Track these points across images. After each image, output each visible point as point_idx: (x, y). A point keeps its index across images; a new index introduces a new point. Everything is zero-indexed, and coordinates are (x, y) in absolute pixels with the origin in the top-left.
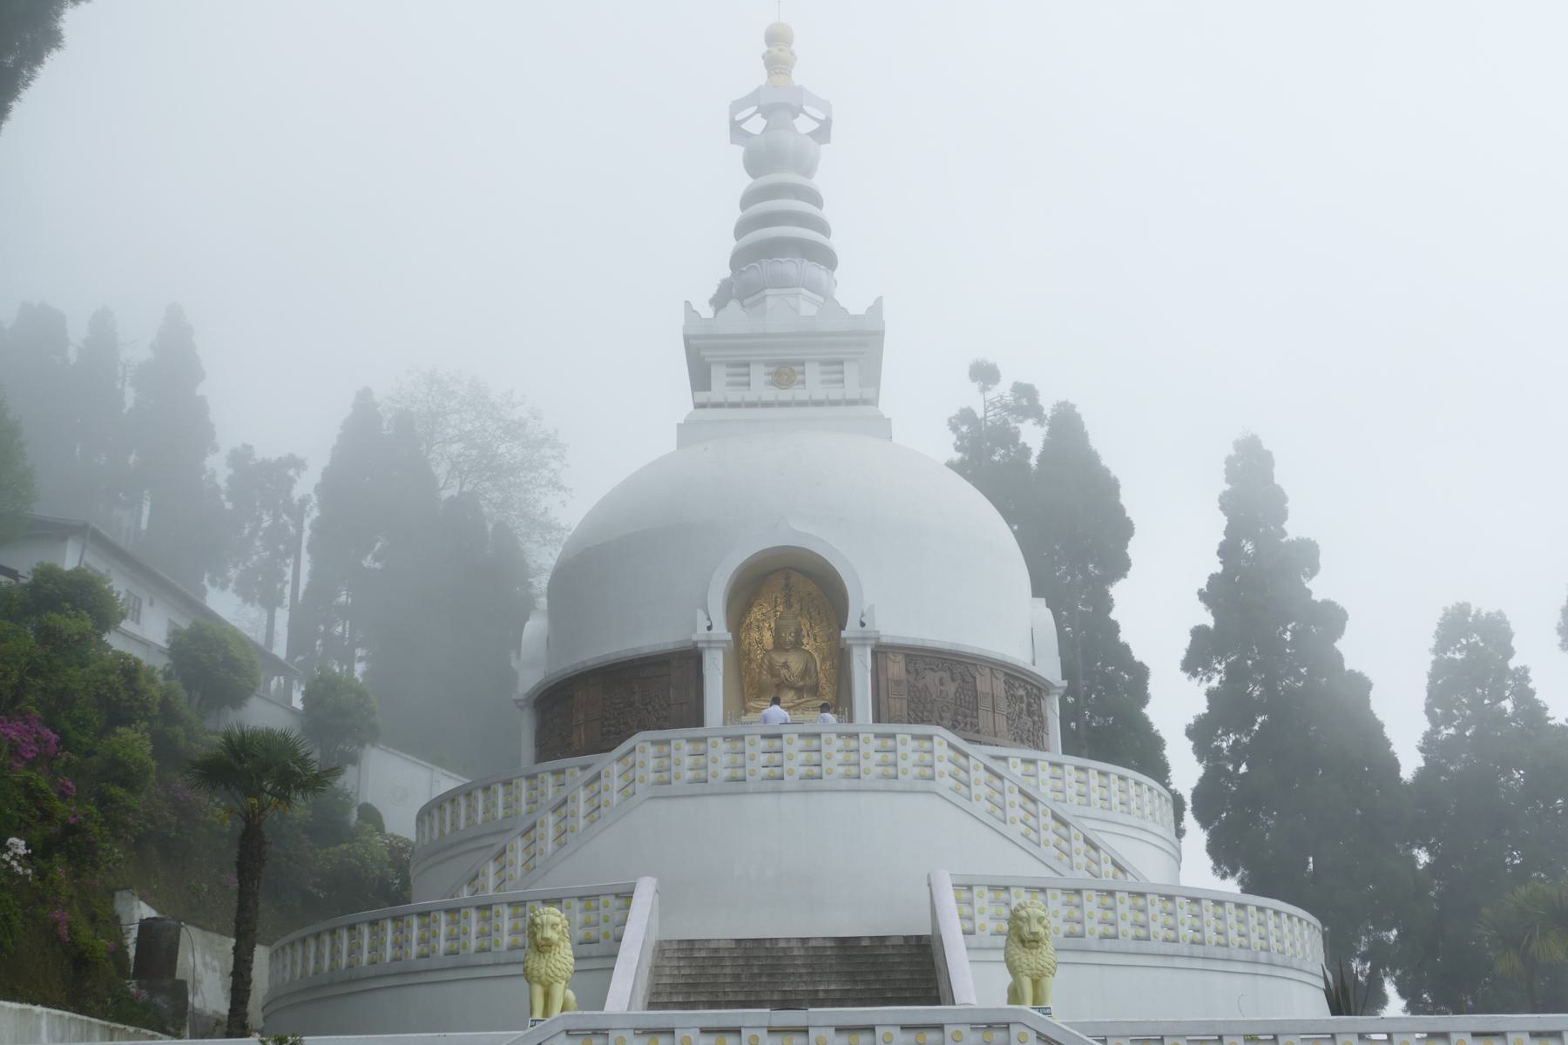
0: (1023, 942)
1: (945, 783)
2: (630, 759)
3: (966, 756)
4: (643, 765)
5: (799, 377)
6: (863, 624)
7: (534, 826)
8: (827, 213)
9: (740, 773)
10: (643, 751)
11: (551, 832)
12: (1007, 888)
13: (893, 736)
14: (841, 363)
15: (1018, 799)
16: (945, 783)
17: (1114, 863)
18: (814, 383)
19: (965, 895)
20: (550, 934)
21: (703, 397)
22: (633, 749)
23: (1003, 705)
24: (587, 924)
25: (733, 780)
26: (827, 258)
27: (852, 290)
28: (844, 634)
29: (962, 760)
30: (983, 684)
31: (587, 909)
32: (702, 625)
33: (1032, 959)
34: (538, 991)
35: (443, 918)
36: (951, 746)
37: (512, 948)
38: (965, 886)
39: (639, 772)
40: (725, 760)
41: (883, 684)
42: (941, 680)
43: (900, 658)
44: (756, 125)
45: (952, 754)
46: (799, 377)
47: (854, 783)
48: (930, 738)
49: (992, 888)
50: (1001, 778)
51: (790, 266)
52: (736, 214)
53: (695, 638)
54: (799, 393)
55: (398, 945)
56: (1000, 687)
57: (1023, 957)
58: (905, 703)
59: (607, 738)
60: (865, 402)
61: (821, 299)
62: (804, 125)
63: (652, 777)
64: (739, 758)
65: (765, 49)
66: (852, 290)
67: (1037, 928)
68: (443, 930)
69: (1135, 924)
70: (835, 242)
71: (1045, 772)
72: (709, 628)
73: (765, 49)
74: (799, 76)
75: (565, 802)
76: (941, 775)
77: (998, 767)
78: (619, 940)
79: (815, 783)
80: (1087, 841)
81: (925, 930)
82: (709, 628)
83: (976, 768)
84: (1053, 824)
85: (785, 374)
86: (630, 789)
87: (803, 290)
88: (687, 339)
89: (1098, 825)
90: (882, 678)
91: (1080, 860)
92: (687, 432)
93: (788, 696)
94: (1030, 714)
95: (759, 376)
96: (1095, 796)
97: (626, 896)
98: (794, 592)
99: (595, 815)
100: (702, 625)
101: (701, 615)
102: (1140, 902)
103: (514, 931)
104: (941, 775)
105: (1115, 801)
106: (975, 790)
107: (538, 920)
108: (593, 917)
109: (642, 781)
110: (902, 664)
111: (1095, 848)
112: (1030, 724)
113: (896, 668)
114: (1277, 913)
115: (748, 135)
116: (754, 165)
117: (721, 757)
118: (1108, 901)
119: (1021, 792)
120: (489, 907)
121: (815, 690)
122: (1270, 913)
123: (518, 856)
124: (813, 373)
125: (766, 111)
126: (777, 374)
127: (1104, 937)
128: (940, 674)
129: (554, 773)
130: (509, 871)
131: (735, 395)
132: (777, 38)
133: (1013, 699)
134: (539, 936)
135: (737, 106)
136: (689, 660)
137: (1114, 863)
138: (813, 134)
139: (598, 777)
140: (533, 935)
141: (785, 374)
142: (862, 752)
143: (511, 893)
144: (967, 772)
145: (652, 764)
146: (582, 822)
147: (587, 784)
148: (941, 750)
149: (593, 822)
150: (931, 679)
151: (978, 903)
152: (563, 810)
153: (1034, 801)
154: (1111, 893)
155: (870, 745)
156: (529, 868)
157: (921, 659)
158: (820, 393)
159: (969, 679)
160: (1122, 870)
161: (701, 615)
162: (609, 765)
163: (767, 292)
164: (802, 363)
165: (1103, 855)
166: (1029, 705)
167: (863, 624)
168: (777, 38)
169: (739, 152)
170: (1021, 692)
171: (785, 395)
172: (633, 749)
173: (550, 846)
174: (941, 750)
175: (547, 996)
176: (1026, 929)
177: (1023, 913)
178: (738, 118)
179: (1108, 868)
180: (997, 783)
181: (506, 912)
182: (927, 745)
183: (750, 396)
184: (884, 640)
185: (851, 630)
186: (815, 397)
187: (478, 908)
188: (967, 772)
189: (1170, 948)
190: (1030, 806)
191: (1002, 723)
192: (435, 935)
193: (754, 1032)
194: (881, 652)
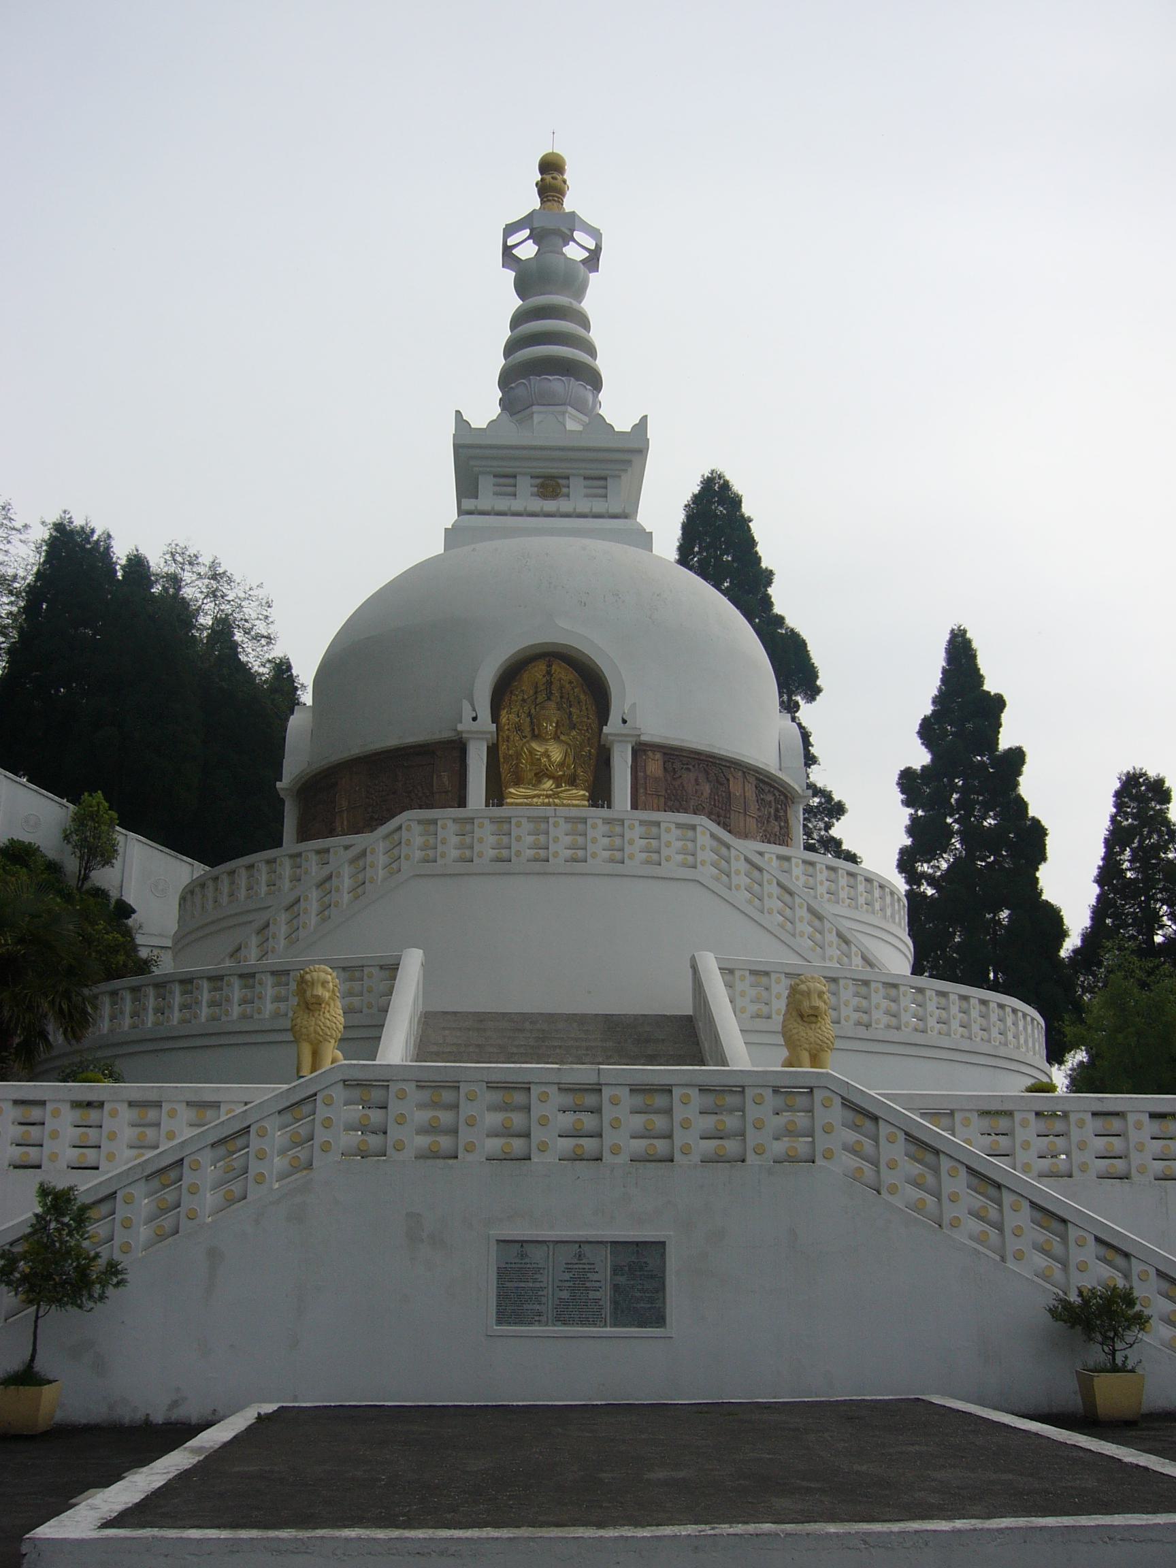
0: (801, 1016)
2: (396, 837)
3: (728, 847)
4: (408, 843)
5: (565, 490)
6: (624, 722)
7: (298, 901)
8: (596, 335)
9: (505, 853)
10: (409, 829)
11: (314, 907)
12: (767, 974)
13: (658, 824)
14: (605, 479)
15: (775, 890)
16: (707, 872)
17: (864, 958)
19: (728, 977)
20: (320, 991)
21: (469, 504)
22: (400, 828)
23: (753, 807)
24: (350, 994)
25: (499, 860)
26: (595, 382)
27: (617, 408)
28: (605, 729)
29: (724, 851)
30: (736, 788)
31: (351, 980)
32: (467, 714)
33: (811, 1033)
34: (306, 1050)
35: (205, 985)
36: (713, 835)
37: (276, 1015)
38: (727, 971)
39: (404, 850)
40: (492, 839)
41: (642, 781)
42: (696, 780)
43: (658, 756)
44: (527, 251)
45: (715, 844)
46: (565, 490)
47: (619, 868)
48: (693, 828)
49: (753, 973)
50: (760, 870)
51: (557, 384)
52: (505, 334)
53: (460, 727)
54: (564, 505)
55: (160, 1011)
56: (751, 792)
57: (800, 1030)
58: (662, 800)
59: (373, 816)
60: (624, 516)
61: (586, 419)
62: (573, 252)
63: (418, 854)
64: (505, 839)
65: (539, 177)
66: (617, 408)
67: (817, 1003)
68: (205, 996)
69: (887, 1012)
70: (602, 364)
71: (798, 870)
72: (475, 719)
73: (539, 177)
74: (570, 204)
75: (330, 877)
76: (703, 863)
77: (756, 859)
78: (385, 1010)
79: (579, 867)
80: (840, 935)
81: (685, 1007)
82: (475, 719)
83: (737, 859)
84: (807, 916)
85: (550, 486)
86: (394, 866)
87: (570, 409)
88: (457, 447)
89: (848, 924)
90: (641, 774)
91: (834, 952)
92: (452, 536)
93: (548, 784)
94: (777, 818)
95: (525, 485)
96: (843, 894)
97: (391, 969)
98: (558, 690)
99: (360, 890)
101: (466, 705)
102: (893, 992)
103: (277, 999)
104: (703, 863)
105: (861, 900)
106: (735, 880)
107: (308, 977)
108: (357, 986)
109: (407, 858)
110: (661, 763)
111: (847, 942)
112: (777, 829)
113: (654, 767)
114: (1014, 1011)
115: (517, 260)
116: (523, 287)
117: (486, 836)
118: (863, 990)
119: (779, 884)
120: (253, 975)
121: (573, 781)
122: (1008, 1010)
123: (281, 929)
124: (577, 486)
125: (536, 236)
126: (542, 486)
127: (859, 1023)
129: (318, 852)
130: (271, 943)
131: (502, 504)
132: (551, 167)
133: (761, 802)
134: (308, 994)
135: (510, 230)
136: (457, 748)
137: (864, 958)
138: (584, 262)
139: (363, 854)
140: (301, 992)
142: (627, 837)
143: (273, 961)
144: (728, 862)
145: (419, 841)
146: (346, 897)
147: (353, 861)
148: (703, 839)
149: (357, 898)
151: (739, 986)
152: (327, 885)
153: (791, 894)
154: (866, 983)
155: (634, 833)
156: (292, 939)
158: (583, 506)
159: (723, 780)
160: (871, 965)
161: (466, 705)
162: (374, 841)
163: (535, 408)
164: (568, 478)
165: (854, 949)
166: (777, 810)
167: (624, 722)
168: (551, 167)
169: (510, 275)
170: (770, 798)
171: (550, 505)
172: (400, 828)
173: (313, 920)
174: (703, 839)
175: (316, 1055)
176: (806, 1004)
177: (803, 987)
178: (510, 243)
179: (857, 961)
180: (756, 873)
181: (269, 980)
182: (690, 834)
183: (517, 505)
184: (644, 738)
185: (612, 727)
186: (579, 510)
187: (241, 976)
188: (728, 862)
189: (919, 1038)
190: (787, 897)
191: (752, 824)
192: (198, 1003)
193: (544, 1089)
194: (641, 750)
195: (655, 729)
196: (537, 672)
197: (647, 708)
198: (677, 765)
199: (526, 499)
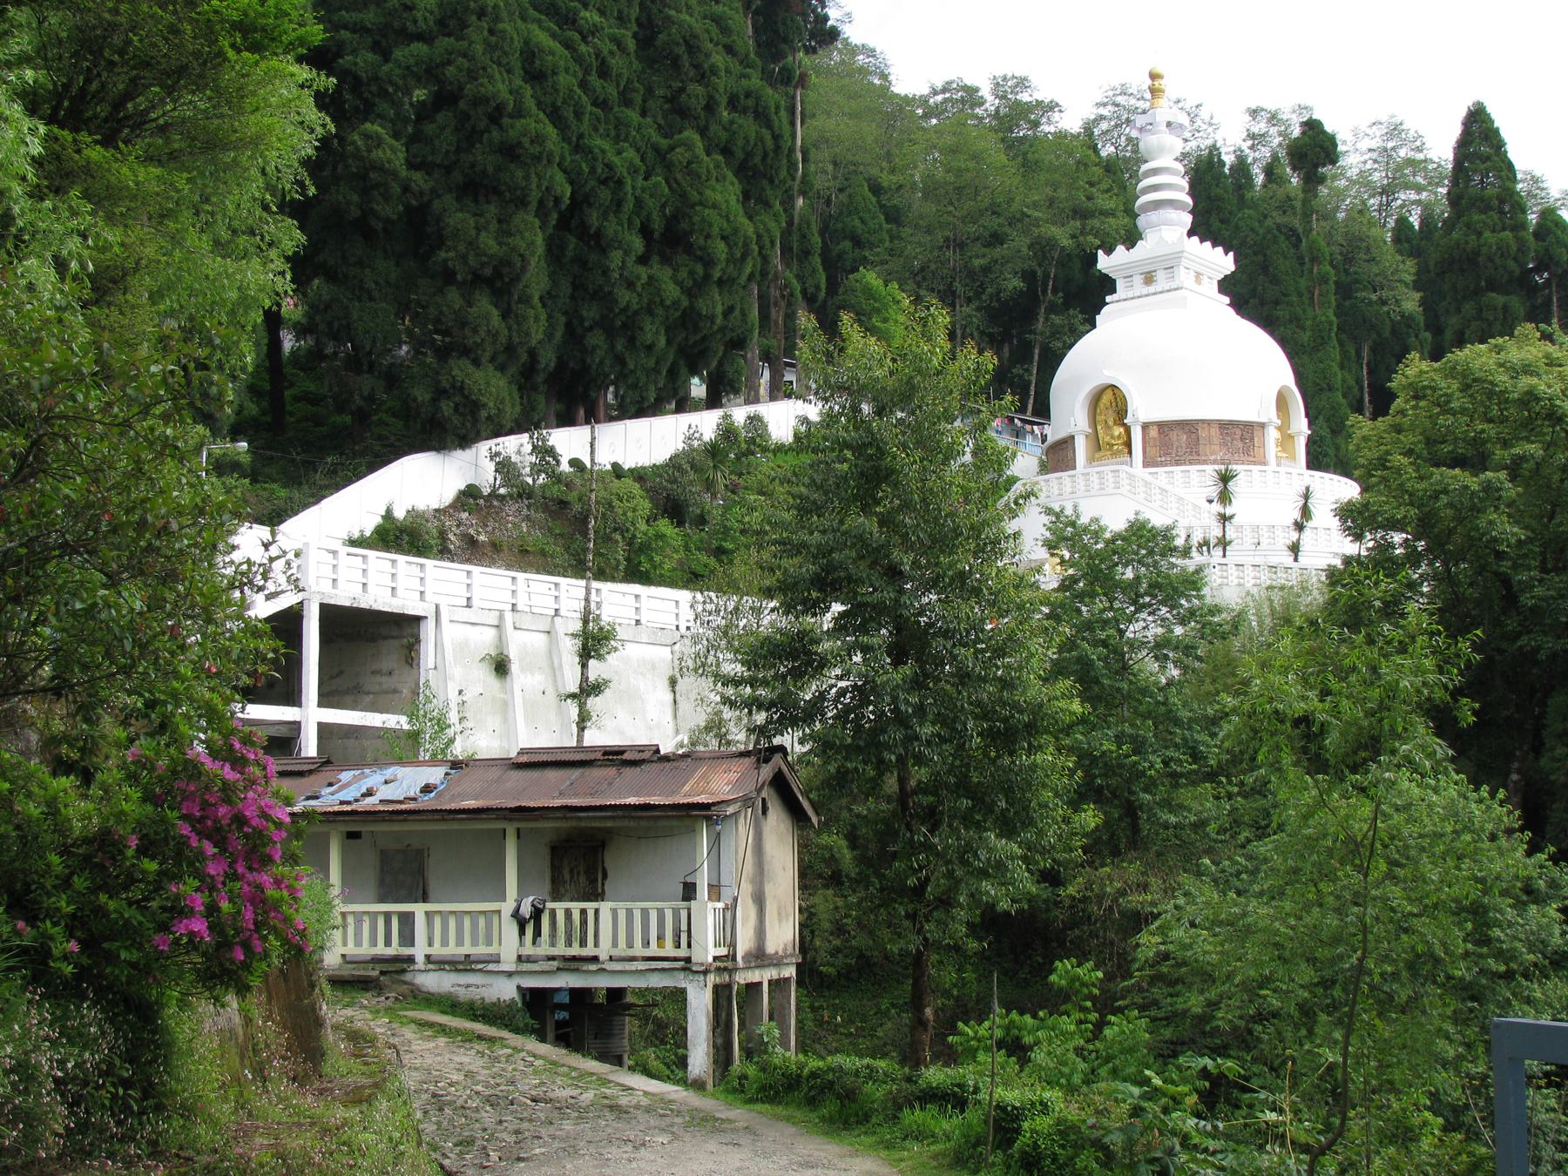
1: (1125, 489)
18: (1162, 282)
30: (1202, 433)
54: (1152, 289)
56: (1215, 431)
85: (1149, 279)
95: (1138, 280)
113: (1153, 432)
124: (1160, 276)
132: (1154, 76)
136: (1073, 437)
141: (1149, 279)
150: (1173, 435)
157: (1164, 426)
171: (1146, 290)
183: (1130, 295)
194: (1145, 427)
195: (1144, 416)
196: (1107, 397)
197: (1144, 408)
199: (1139, 287)
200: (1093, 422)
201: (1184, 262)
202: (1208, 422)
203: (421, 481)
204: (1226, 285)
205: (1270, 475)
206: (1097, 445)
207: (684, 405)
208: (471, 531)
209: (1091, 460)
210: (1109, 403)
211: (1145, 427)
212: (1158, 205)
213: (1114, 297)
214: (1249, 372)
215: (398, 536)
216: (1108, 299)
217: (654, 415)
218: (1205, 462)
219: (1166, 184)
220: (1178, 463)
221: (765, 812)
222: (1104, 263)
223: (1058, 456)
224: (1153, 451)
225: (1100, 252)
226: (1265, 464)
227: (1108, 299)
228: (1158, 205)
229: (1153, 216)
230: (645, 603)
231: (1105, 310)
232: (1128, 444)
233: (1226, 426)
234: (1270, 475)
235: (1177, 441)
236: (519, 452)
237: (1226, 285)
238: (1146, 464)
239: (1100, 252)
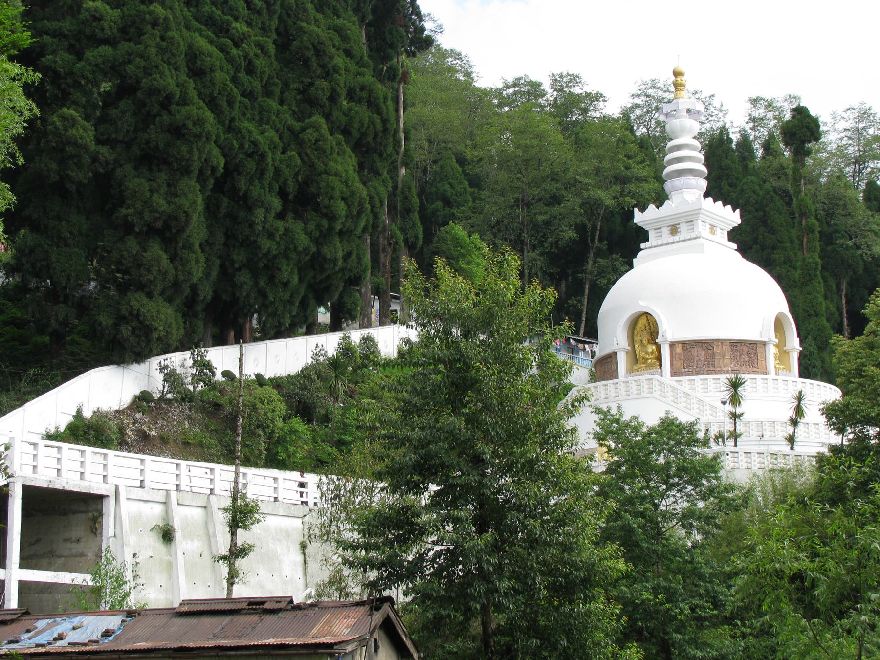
1: (656, 394)
30: (717, 349)
54: (676, 238)
56: (726, 348)
85: (674, 230)
94: (748, 354)
95: (665, 231)
100: (615, 344)
113: (679, 349)
124: (683, 228)
128: (695, 349)
132: (676, 74)
136: (615, 354)
150: (694, 352)
157: (687, 345)
171: (671, 239)
183: (660, 243)
194: (672, 345)
196: (642, 322)
197: (671, 331)
198: (688, 347)
199: (666, 237)
200: (632, 342)
201: (702, 217)
202: (722, 341)
203: (104, 389)
204: (734, 235)
205: (770, 382)
206: (635, 360)
207: (312, 329)
208: (145, 428)
209: (630, 371)
210: (644, 326)
211: (672, 345)
212: (680, 173)
213: (647, 244)
214: (750, 301)
215: (86, 431)
216: (642, 246)
217: (289, 336)
218: (719, 372)
219: (687, 155)
220: (698, 373)
221: (376, 649)
222: (639, 218)
223: (604, 368)
224: (678, 364)
225: (636, 210)
226: (766, 373)
227: (642, 246)
228: (680, 173)
229: (677, 182)
230: (281, 484)
231: (640, 254)
232: (659, 359)
233: (735, 344)
234: (770, 382)
235: (697, 356)
236: (183, 365)
237: (734, 235)
238: (673, 374)
239: (636, 210)
